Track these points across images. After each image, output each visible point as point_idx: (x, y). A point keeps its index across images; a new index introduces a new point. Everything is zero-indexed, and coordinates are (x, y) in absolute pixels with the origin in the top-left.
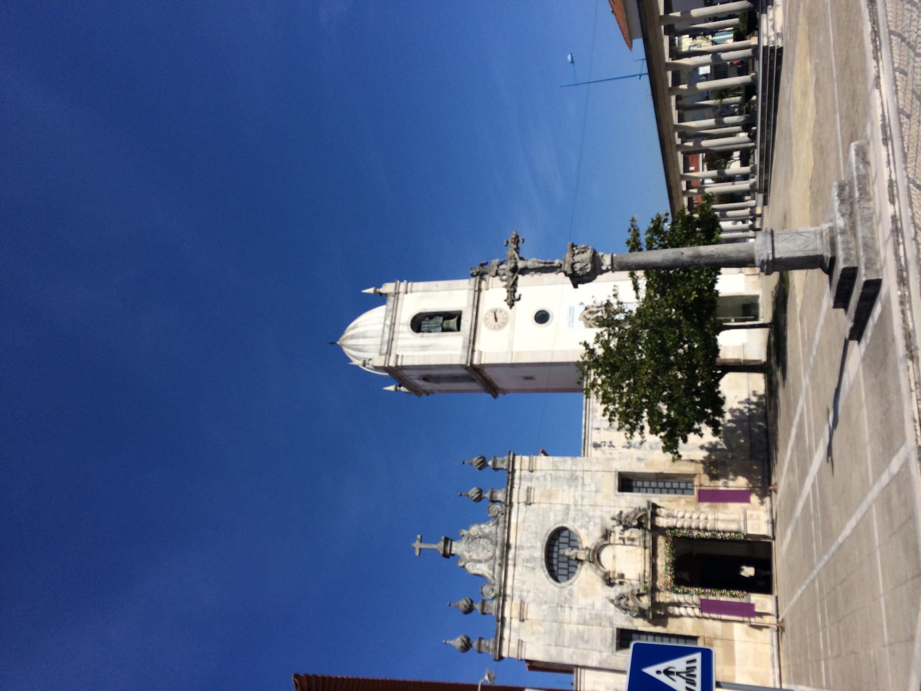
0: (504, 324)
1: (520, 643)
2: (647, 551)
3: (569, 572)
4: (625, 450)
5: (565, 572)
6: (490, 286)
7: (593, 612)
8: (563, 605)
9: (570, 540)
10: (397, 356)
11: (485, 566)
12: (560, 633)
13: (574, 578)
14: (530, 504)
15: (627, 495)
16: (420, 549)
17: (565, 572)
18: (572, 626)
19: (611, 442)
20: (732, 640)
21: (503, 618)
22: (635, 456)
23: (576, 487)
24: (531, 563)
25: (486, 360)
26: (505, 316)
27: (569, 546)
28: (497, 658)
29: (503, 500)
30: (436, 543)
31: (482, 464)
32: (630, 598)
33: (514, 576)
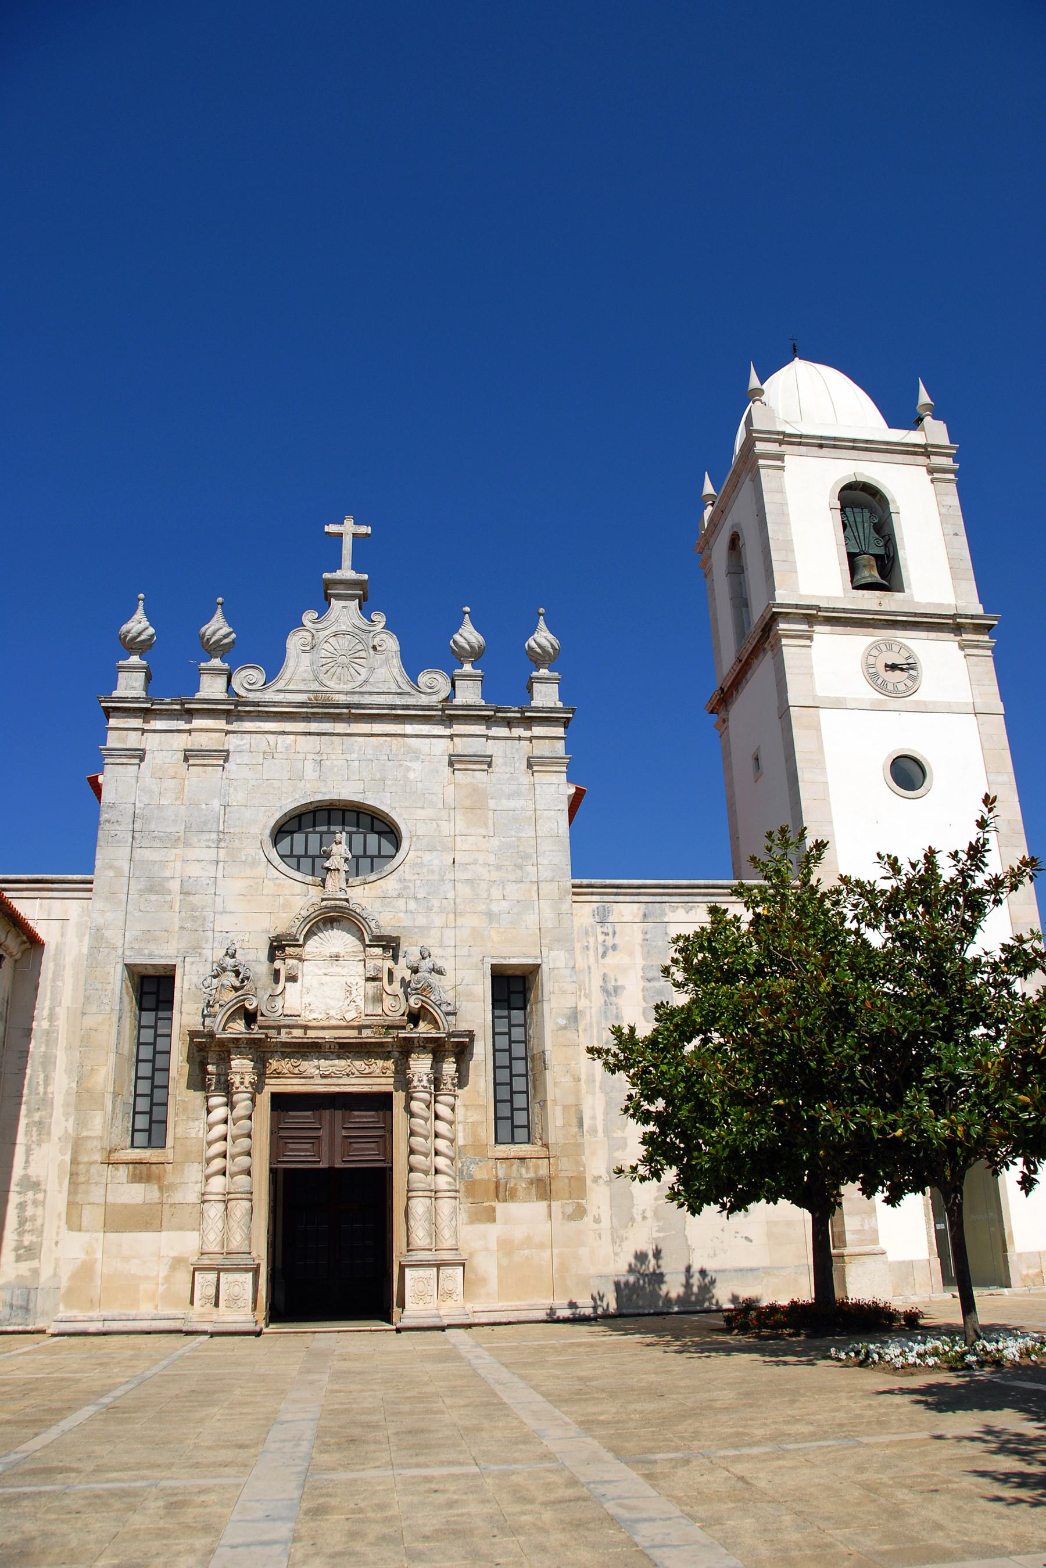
0: (881, 687)
1: (140, 755)
2: (354, 1033)
3: (299, 857)
4: (601, 983)
5: (299, 850)
6: (969, 651)
7: (208, 913)
8: (222, 844)
9: (372, 857)
10: (780, 457)
11: (306, 671)
12: (161, 839)
13: (283, 867)
14: (451, 764)
15: (484, 989)
16: (341, 535)
17: (299, 850)
18: (178, 864)
19: (614, 947)
20: (160, 1229)
21: (190, 714)
22: (582, 1004)
23: (499, 868)
24: (315, 771)
25: (791, 652)
26: (901, 687)
27: (357, 857)
28: (103, 705)
29: (458, 701)
30: (355, 567)
31: (538, 650)
32: (240, 993)
33: (284, 733)
